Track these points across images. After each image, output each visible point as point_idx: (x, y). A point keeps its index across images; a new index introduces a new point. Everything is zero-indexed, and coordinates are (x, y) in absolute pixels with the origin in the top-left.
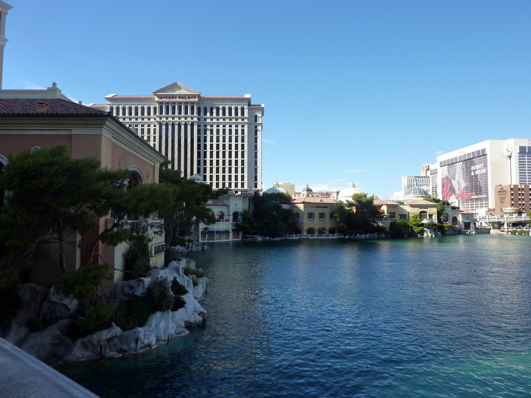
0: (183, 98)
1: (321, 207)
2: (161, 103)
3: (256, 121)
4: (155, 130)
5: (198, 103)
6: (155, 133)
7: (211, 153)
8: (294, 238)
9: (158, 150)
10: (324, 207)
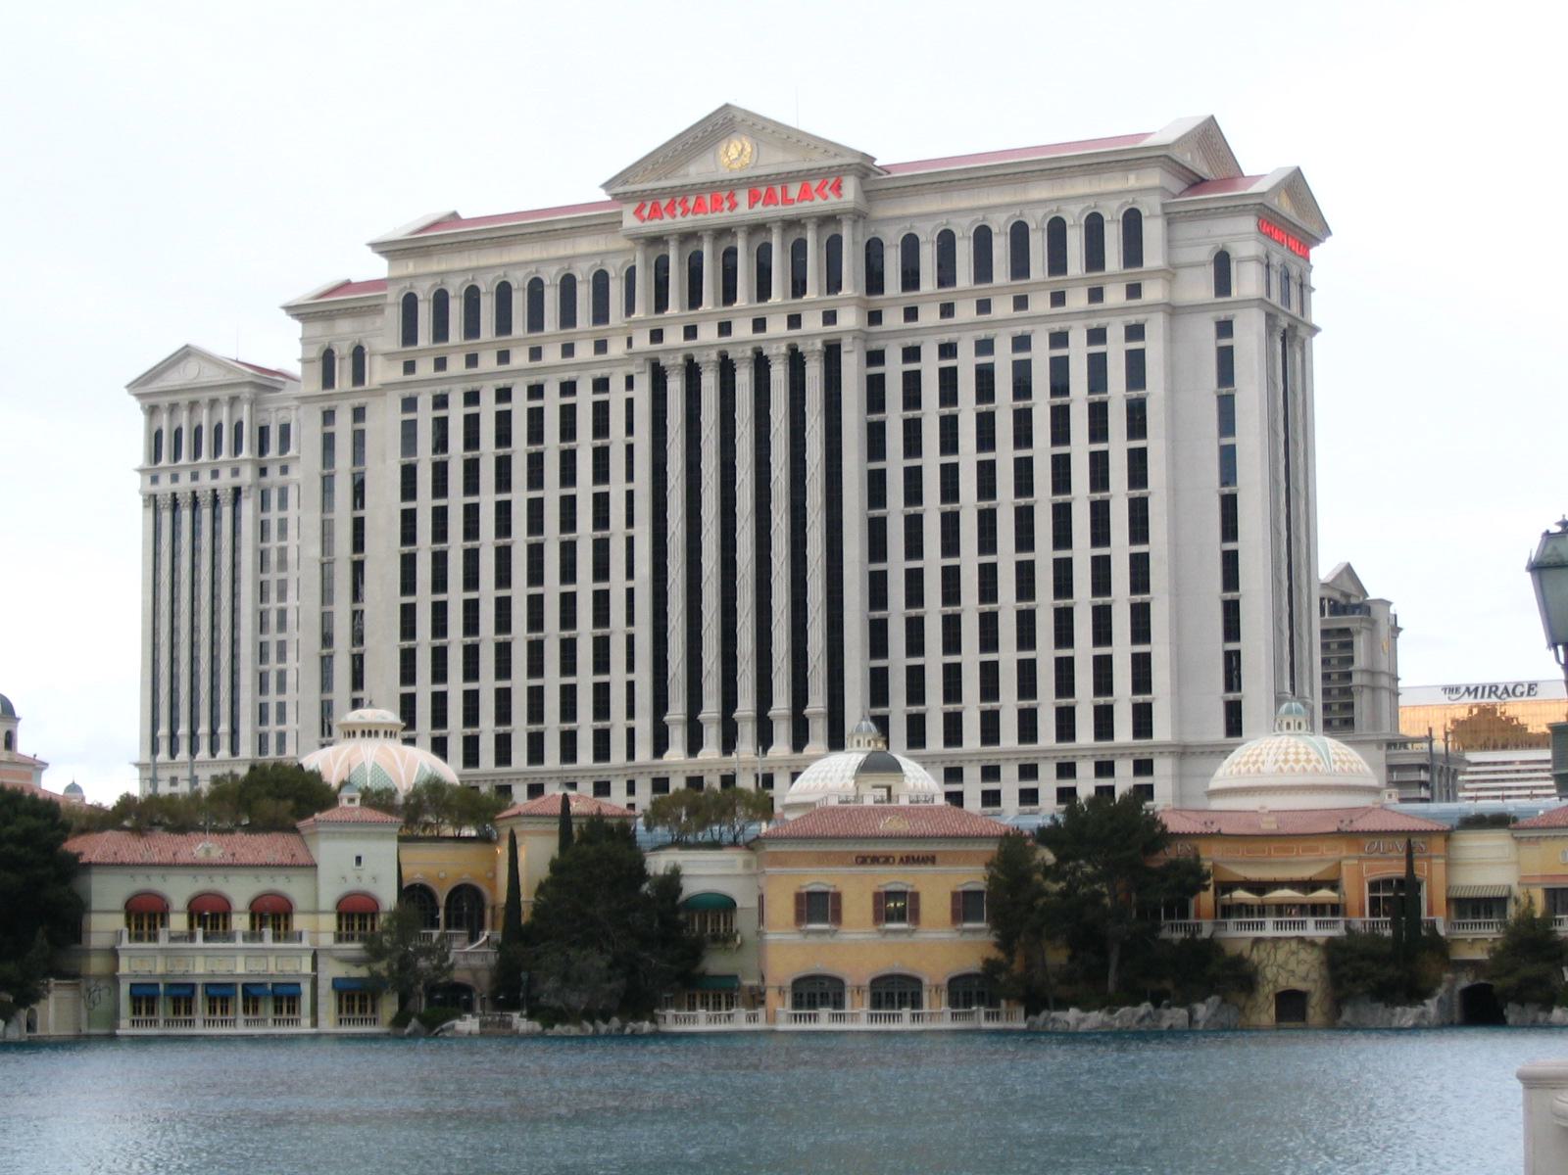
0: (770, 198)
1: (887, 860)
2: (656, 240)
3: (1223, 285)
5: (859, 216)
7: (914, 525)
8: (702, 1026)
10: (909, 860)
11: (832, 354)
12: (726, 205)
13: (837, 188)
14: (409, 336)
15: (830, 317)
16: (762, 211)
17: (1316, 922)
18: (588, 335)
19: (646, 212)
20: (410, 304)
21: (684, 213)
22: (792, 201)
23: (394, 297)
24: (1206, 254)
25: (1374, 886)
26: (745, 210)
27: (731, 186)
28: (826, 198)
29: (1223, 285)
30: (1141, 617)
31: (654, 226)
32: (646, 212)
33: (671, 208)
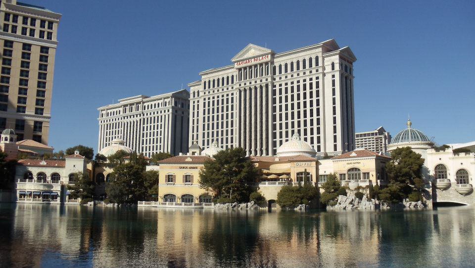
2: (240, 69)
3: (333, 68)
11: (267, 86)
14: (205, 88)
15: (267, 80)
17: (279, 183)
20: (205, 82)
23: (203, 82)
24: (330, 63)
25: (298, 174)
26: (253, 62)
27: (251, 58)
29: (333, 68)
31: (239, 67)
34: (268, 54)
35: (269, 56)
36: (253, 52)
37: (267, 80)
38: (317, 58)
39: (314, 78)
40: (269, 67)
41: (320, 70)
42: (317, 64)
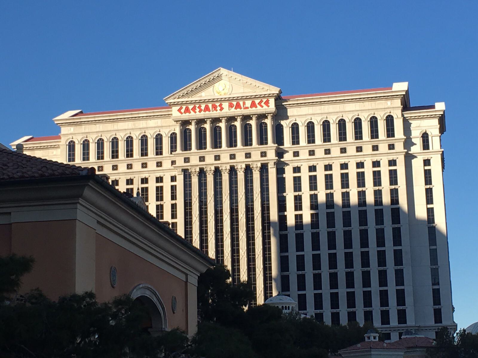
0: (238, 106)
2: (185, 123)
4: (173, 189)
6: (174, 197)
9: (198, 246)
12: (219, 108)
13: (267, 103)
16: (233, 112)
18: (154, 159)
19: (183, 111)
21: (200, 111)
22: (247, 108)
23: (63, 142)
28: (262, 107)
30: (399, 274)
31: (186, 116)
32: (183, 111)
33: (194, 109)
34: (269, 96)
35: (272, 101)
36: (231, 89)
37: (263, 154)
38: (390, 120)
39: (384, 163)
40: (271, 127)
41: (399, 147)
42: (390, 132)
